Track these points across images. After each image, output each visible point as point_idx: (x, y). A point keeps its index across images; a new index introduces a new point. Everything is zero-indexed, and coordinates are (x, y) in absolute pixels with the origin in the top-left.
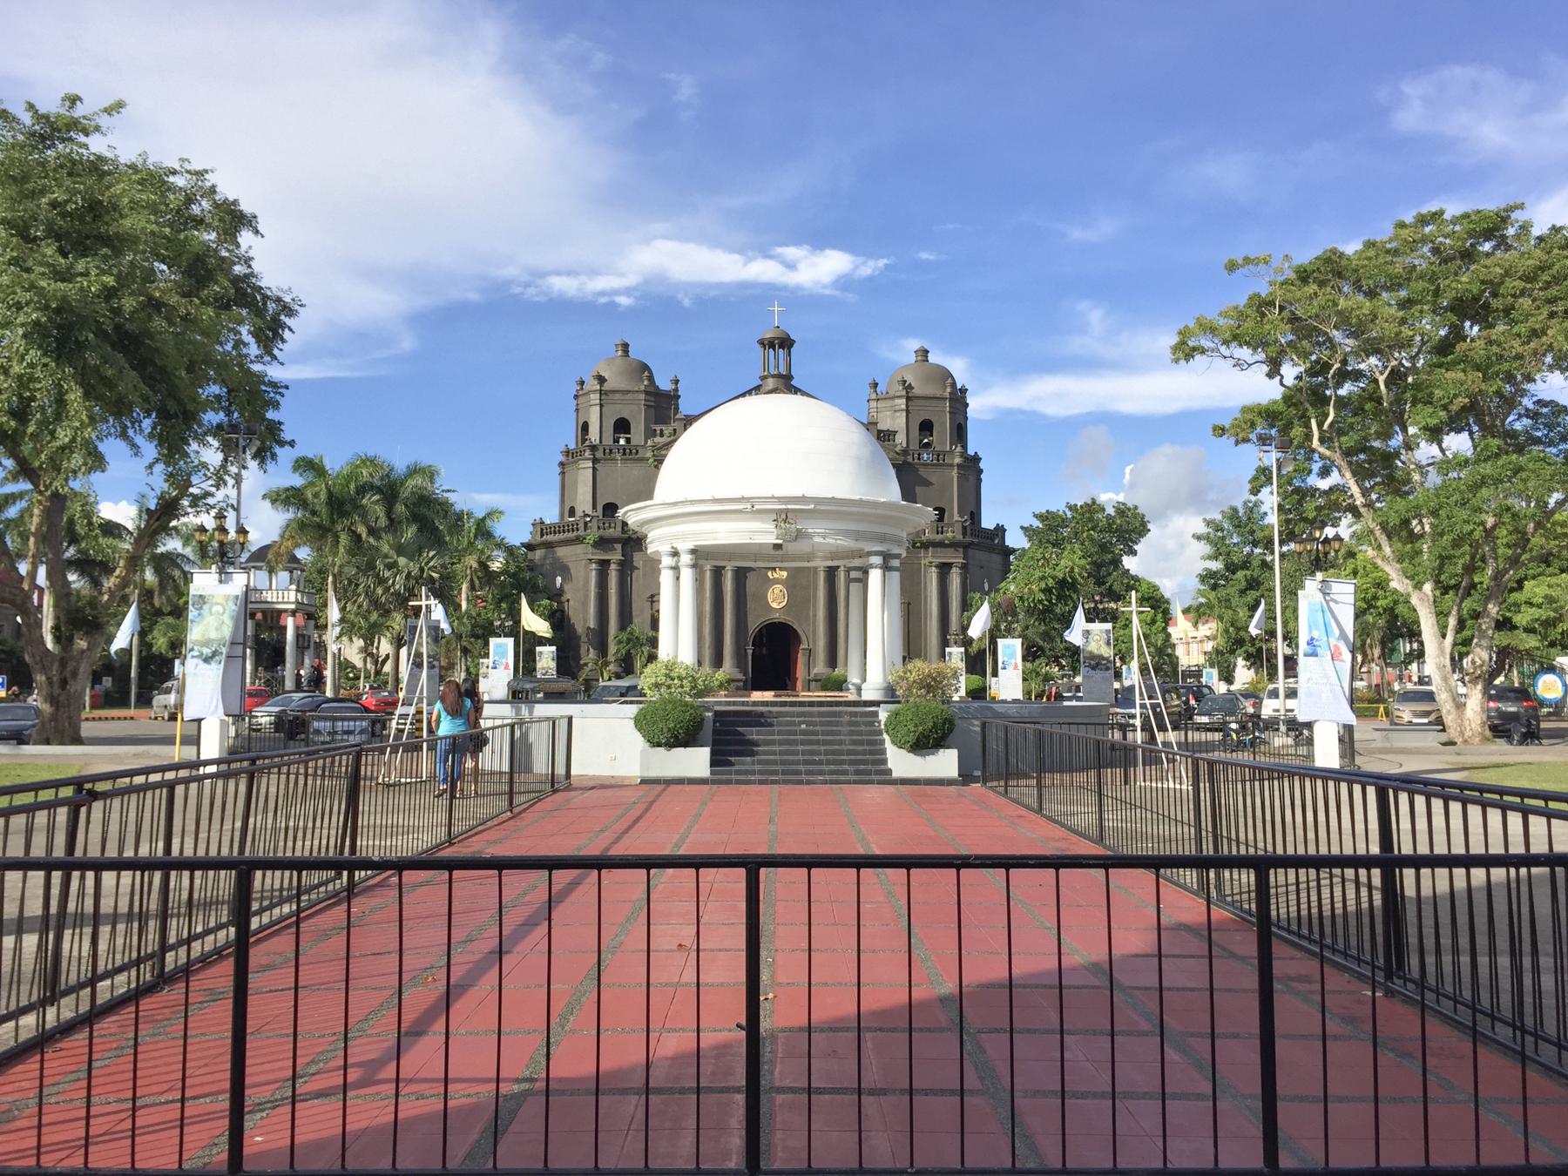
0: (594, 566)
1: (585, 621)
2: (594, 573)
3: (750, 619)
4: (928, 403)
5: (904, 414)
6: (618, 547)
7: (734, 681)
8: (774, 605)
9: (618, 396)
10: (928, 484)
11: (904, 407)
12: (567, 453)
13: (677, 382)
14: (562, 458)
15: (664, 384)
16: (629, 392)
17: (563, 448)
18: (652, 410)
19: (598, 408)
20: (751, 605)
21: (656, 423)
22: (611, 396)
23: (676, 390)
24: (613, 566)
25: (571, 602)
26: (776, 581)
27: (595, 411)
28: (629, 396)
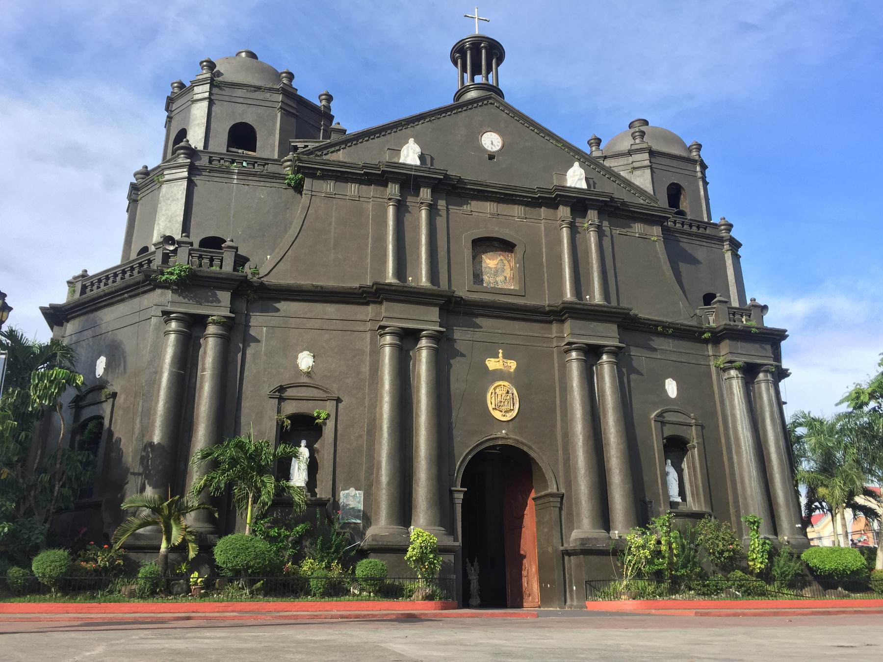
0: (174, 325)
1: (147, 429)
2: (172, 337)
3: (458, 435)
4: (675, 163)
5: (648, 172)
6: (225, 297)
7: (441, 550)
8: (497, 415)
9: (239, 93)
10: (694, 261)
11: (647, 163)
13: (329, 98)
16: (258, 88)
17: (139, 168)
18: (293, 120)
19: (205, 104)
20: (458, 413)
21: (297, 137)
22: (227, 91)
23: (329, 108)
24: (211, 329)
25: (121, 399)
26: (499, 375)
27: (199, 111)
28: (258, 95)
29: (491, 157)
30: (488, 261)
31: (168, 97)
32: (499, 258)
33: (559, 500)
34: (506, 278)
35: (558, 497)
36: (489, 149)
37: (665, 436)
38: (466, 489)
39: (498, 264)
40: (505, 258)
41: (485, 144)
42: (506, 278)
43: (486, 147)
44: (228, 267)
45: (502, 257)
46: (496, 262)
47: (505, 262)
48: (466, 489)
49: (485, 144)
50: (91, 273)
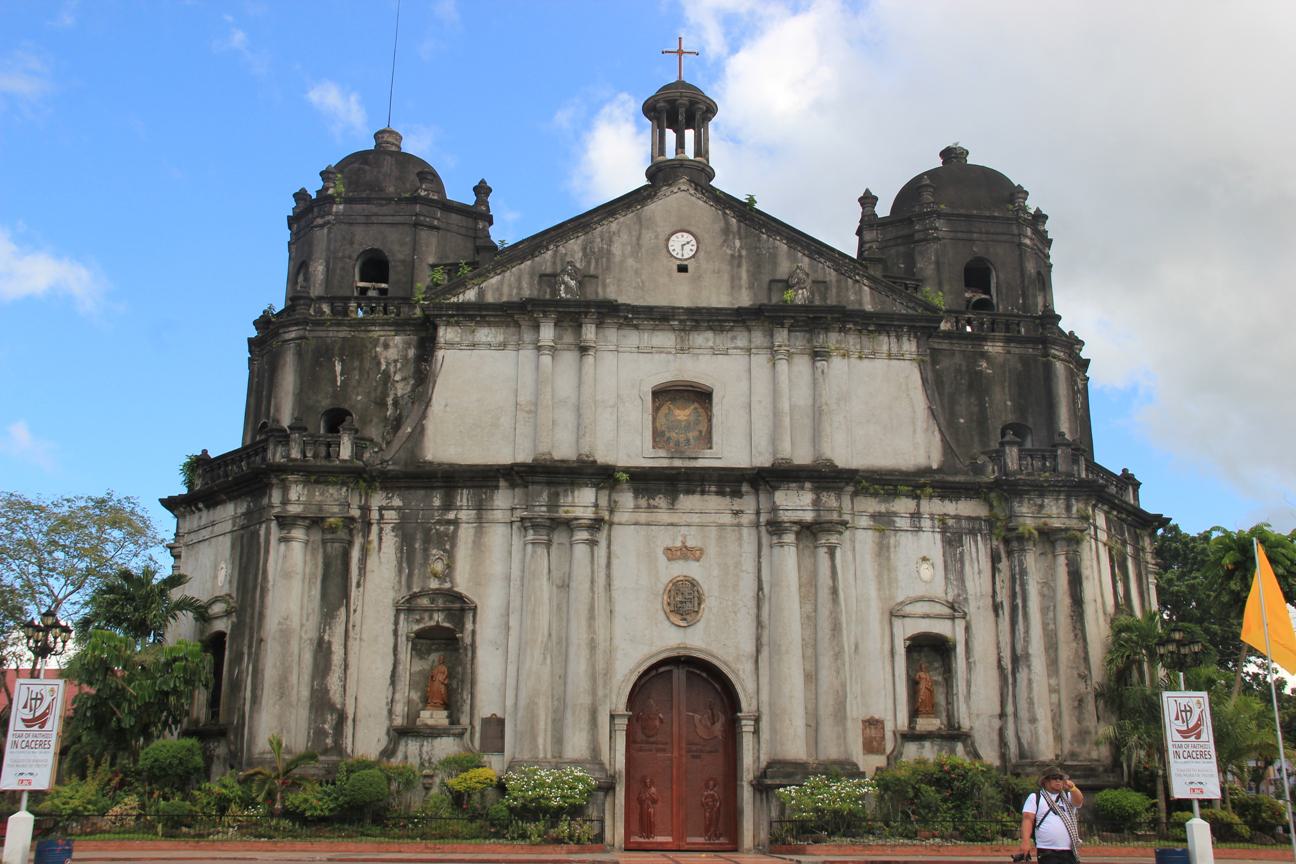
12: (265, 323)
14: (254, 333)
15: (459, 192)
29: (683, 269)
30: (677, 412)
31: (288, 217)
32: (692, 407)
33: (752, 723)
34: (701, 432)
35: (751, 720)
36: (679, 256)
37: (909, 633)
38: (631, 713)
39: (690, 414)
40: (701, 405)
41: (674, 250)
42: (701, 432)
43: (674, 254)
44: (346, 451)
45: (696, 405)
46: (687, 412)
47: (700, 410)
48: (631, 713)
49: (674, 250)
50: (213, 454)
